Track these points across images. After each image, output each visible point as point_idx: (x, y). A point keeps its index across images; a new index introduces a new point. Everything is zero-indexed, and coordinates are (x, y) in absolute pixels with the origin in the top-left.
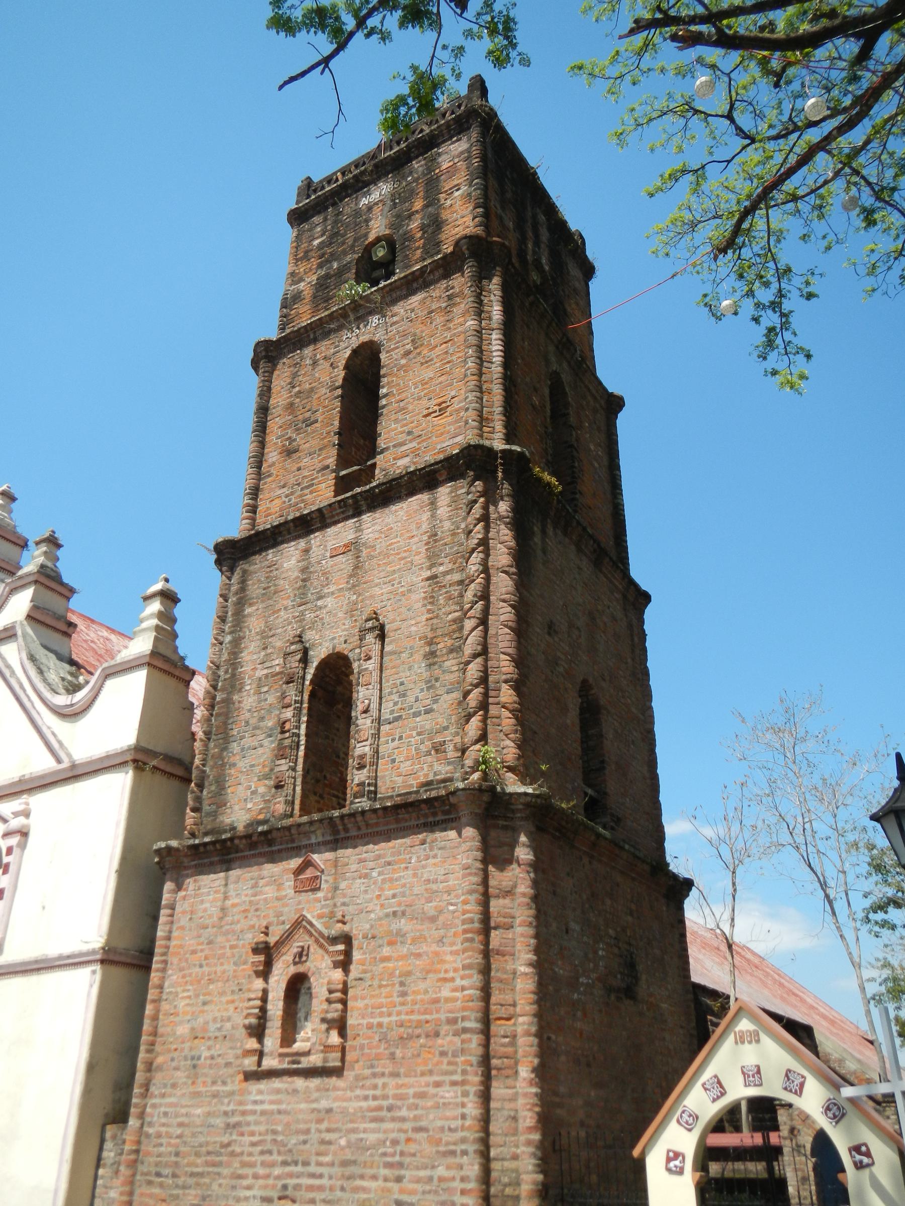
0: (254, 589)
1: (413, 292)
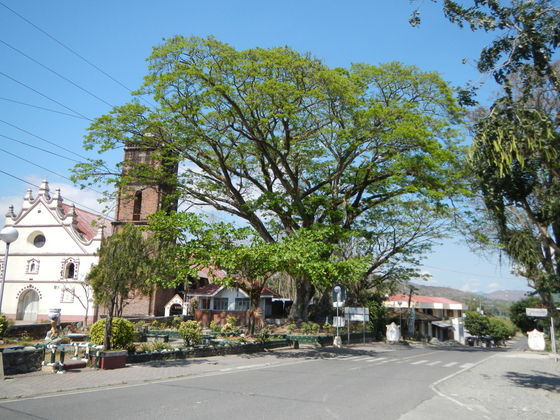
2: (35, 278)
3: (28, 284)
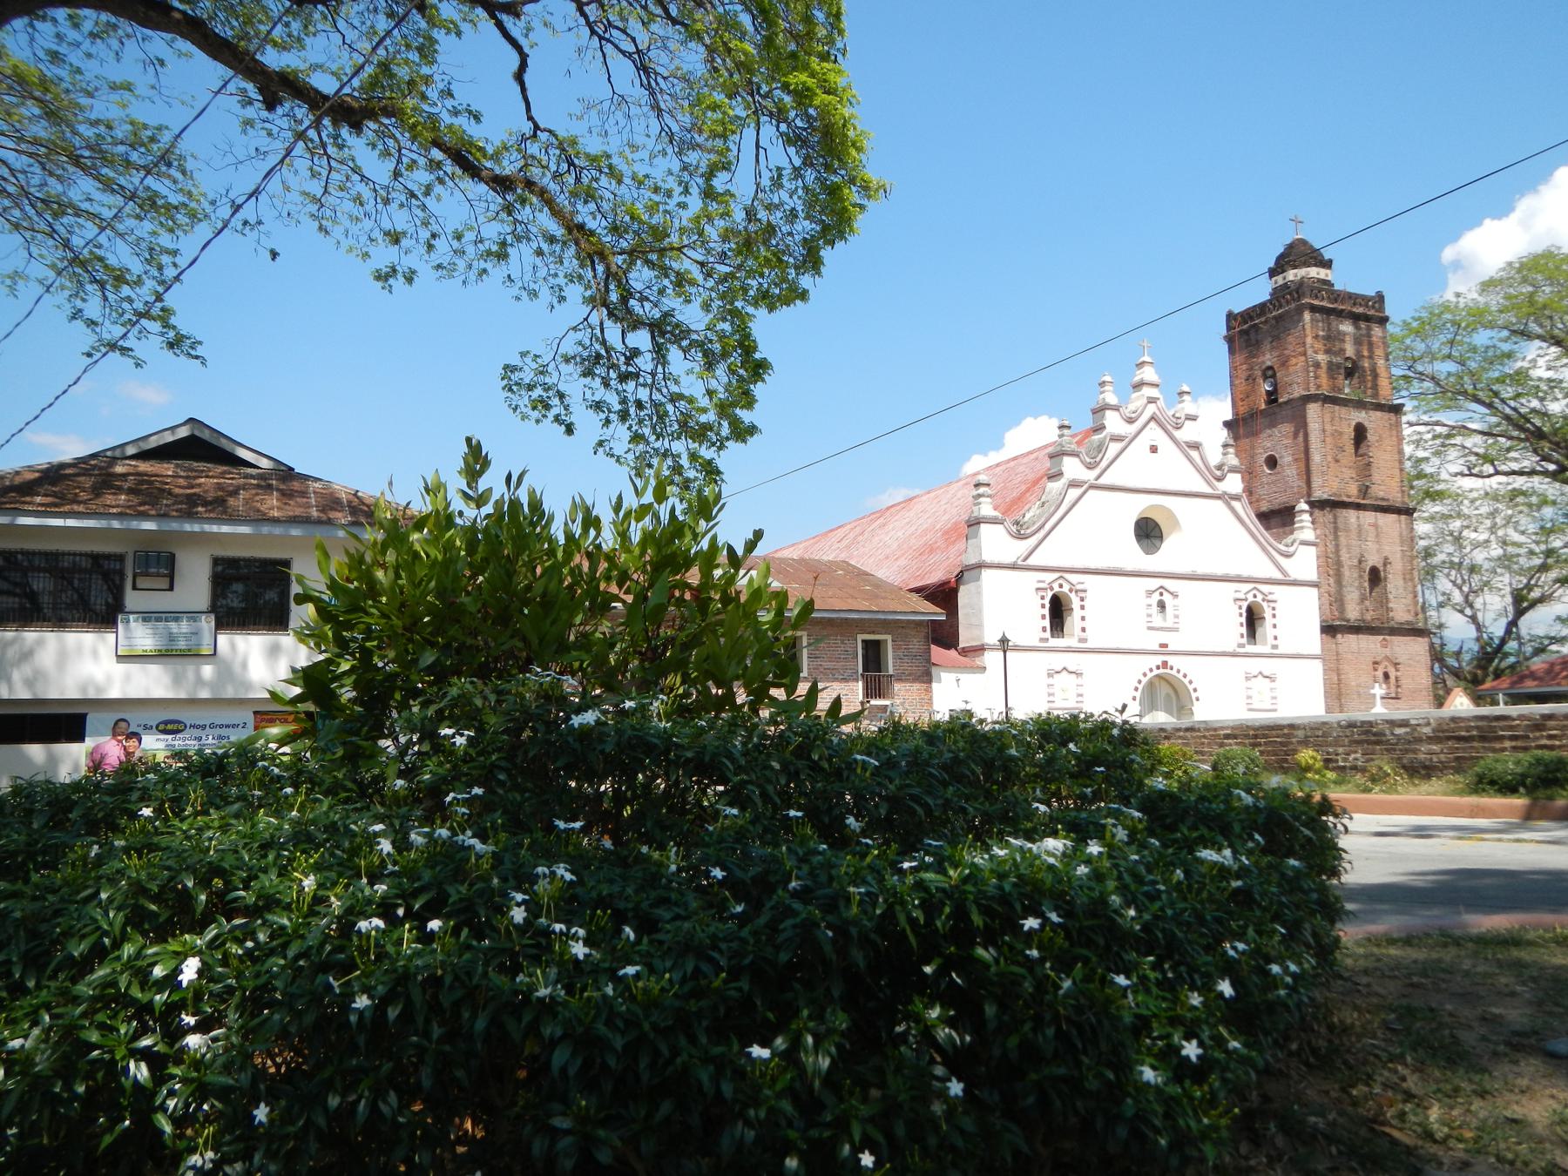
0: (1341, 525)
3: (1159, 660)
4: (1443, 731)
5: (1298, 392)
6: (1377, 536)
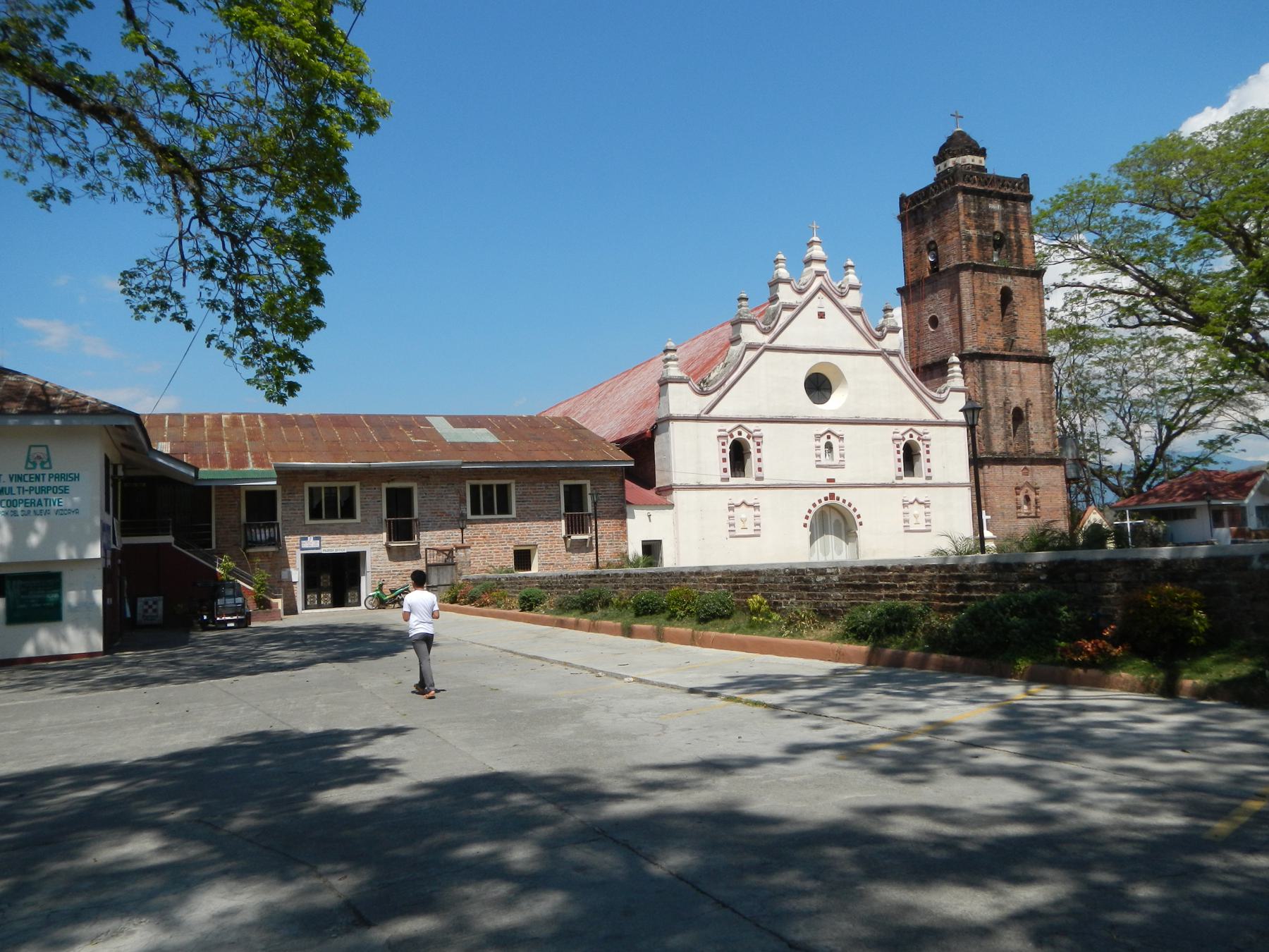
0: (988, 373)
1: (1021, 275)
2: (840, 476)
3: (826, 492)
4: (846, 580)
5: (954, 262)
6: (1021, 381)
